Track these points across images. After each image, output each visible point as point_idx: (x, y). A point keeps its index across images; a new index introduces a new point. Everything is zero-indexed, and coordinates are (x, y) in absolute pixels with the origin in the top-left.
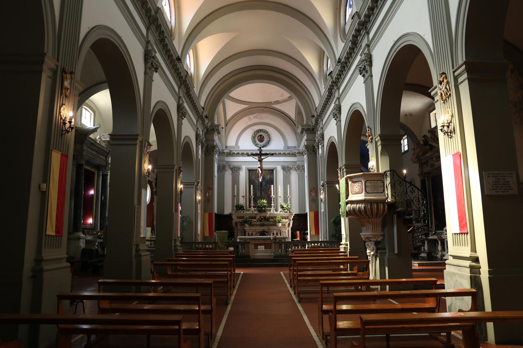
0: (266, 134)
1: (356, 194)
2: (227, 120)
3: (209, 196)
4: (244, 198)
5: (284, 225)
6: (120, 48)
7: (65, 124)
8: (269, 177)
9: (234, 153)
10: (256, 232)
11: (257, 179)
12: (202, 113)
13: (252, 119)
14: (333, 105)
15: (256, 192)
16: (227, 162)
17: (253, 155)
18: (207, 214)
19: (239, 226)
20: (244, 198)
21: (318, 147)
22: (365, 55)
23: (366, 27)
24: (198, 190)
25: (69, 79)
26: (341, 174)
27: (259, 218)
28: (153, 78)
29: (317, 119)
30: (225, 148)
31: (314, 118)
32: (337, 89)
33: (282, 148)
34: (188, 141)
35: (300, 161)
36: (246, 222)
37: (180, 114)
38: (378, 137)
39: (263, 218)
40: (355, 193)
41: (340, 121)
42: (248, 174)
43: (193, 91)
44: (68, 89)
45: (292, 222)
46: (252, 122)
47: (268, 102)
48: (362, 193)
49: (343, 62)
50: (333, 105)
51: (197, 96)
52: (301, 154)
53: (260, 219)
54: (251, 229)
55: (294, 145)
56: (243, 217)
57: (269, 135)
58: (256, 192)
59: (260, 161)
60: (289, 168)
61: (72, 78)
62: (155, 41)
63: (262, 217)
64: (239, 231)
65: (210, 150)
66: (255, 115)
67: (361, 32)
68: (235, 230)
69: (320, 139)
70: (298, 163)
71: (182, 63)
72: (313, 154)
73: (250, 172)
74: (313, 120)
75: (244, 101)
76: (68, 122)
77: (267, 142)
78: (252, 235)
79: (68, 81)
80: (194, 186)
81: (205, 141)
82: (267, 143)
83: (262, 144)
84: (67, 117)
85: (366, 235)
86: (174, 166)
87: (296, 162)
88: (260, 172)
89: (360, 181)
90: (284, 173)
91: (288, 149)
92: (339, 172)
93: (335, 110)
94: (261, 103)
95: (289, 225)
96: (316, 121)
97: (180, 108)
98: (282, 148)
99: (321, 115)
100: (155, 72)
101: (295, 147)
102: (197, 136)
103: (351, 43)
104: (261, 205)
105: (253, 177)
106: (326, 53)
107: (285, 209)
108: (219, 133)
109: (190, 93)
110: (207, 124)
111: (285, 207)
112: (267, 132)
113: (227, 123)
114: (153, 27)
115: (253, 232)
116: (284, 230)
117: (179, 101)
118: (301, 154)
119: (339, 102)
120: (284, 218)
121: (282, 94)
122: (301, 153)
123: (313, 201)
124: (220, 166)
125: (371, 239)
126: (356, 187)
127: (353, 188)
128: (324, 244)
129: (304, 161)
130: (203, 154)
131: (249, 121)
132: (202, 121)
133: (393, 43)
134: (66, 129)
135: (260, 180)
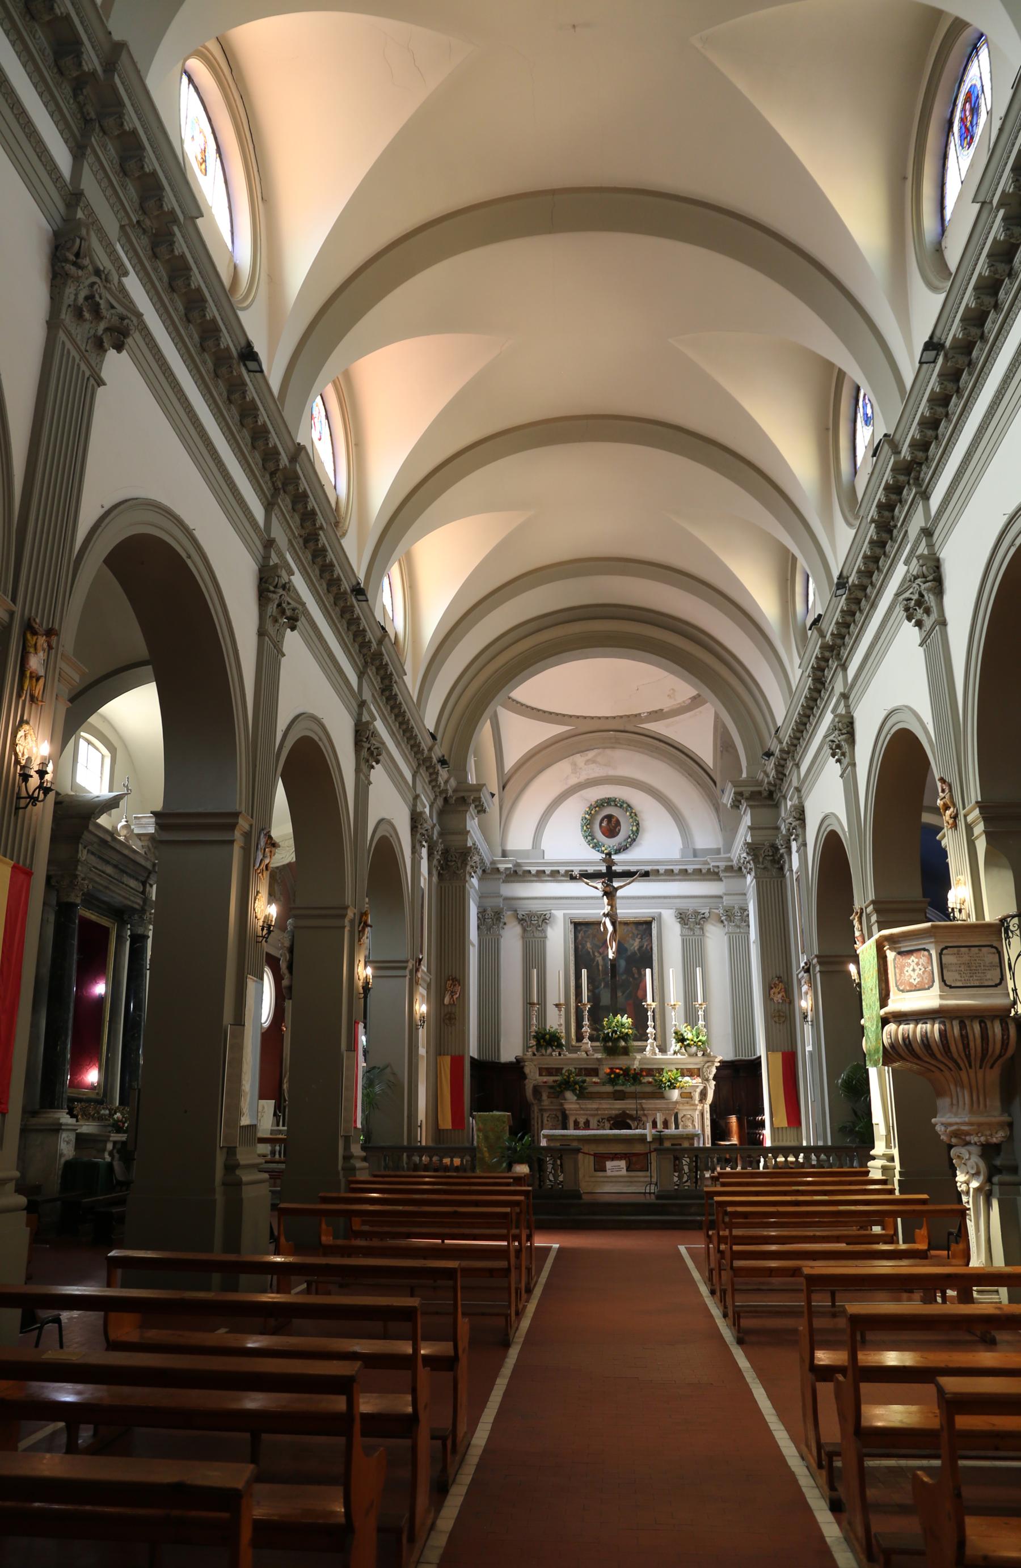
1: (911, 991)
2: (506, 772)
3: (452, 1004)
4: (560, 1011)
5: (687, 1096)
6: (189, 562)
7: (26, 777)
9: (529, 872)
11: (601, 950)
12: (430, 749)
13: (581, 769)
14: (828, 718)
15: (597, 991)
16: (506, 899)
17: (586, 876)
18: (447, 1060)
19: (545, 1097)
20: (560, 1011)
21: (789, 848)
22: (921, 561)
23: (917, 479)
24: (417, 983)
25: (44, 650)
26: (862, 930)
27: (609, 1074)
28: (282, 647)
29: (782, 762)
30: (500, 854)
31: (773, 760)
32: (839, 669)
33: (676, 855)
34: (388, 835)
36: (567, 1085)
37: (364, 753)
38: (975, 809)
39: (621, 1072)
40: (908, 988)
41: (854, 765)
42: (571, 936)
43: (401, 683)
44: (38, 679)
45: (713, 1088)
46: (583, 777)
47: (628, 716)
48: (932, 986)
49: (854, 585)
50: (828, 718)
51: (415, 700)
52: (736, 871)
53: (613, 1076)
54: (582, 1109)
55: (714, 846)
56: (558, 1071)
57: (634, 816)
58: (597, 991)
59: (610, 894)
60: (699, 917)
61: (50, 647)
62: (290, 541)
63: (618, 1071)
64: (546, 1115)
65: (453, 863)
66: (591, 754)
67: (905, 492)
68: (534, 1111)
69: (794, 824)
70: (727, 901)
71: (370, 602)
72: (774, 872)
73: (579, 928)
74: (771, 765)
75: (557, 714)
76: (37, 772)
77: (630, 837)
78: (587, 1126)
79: (41, 654)
80: (407, 972)
81: (441, 834)
82: (629, 840)
83: (612, 843)
84: (33, 759)
85: (951, 1125)
86: (346, 908)
87: (721, 897)
88: (610, 928)
89: (924, 950)
90: (686, 932)
91: (695, 856)
92: (856, 923)
93: (837, 732)
94: (607, 718)
95: (703, 1094)
96: (780, 769)
97: (362, 734)
98: (676, 855)
99: (792, 748)
100: (289, 630)
101: (718, 851)
102: (416, 820)
103: (875, 527)
104: (615, 1032)
106: (801, 562)
107: (689, 1045)
108: (481, 810)
109: (391, 690)
110: (446, 782)
111: (688, 1039)
112: (629, 806)
113: (505, 781)
114: (283, 500)
115: (590, 1118)
116: (690, 1113)
117: (360, 714)
118: (736, 871)
119: (847, 706)
120: (686, 1073)
121: (673, 689)
122: (736, 868)
123: (777, 1019)
124: (485, 911)
125: (968, 1138)
126: (911, 968)
127: (902, 972)
128: (818, 1157)
129: (745, 894)
130: (435, 873)
131: (572, 773)
132: (431, 774)
133: (1004, 520)
134: (31, 794)
135: (611, 956)
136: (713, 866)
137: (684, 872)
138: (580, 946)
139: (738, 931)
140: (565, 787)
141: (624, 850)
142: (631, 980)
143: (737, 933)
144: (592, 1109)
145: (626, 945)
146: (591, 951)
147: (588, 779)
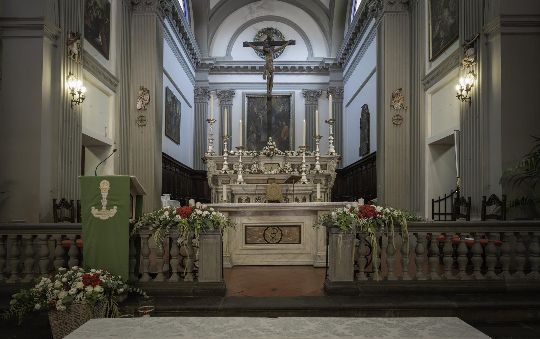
0: (279, 35)
8: (281, 108)
10: (255, 197)
15: (259, 134)
16: (210, 84)
35: (336, 81)
46: (255, 16)
54: (244, 190)
58: (259, 134)
60: (316, 94)
68: (213, 193)
70: (332, 84)
73: (250, 100)
78: (248, 201)
105: (255, 109)
115: (250, 197)
129: (342, 81)
136: (326, 64)
137: (309, 68)
138: (251, 110)
139: (337, 101)
140: (245, 22)
141: (277, 57)
142: (278, 128)
143: (336, 102)
144: (252, 190)
145: (275, 109)
146: (255, 111)
147: (258, 17)
